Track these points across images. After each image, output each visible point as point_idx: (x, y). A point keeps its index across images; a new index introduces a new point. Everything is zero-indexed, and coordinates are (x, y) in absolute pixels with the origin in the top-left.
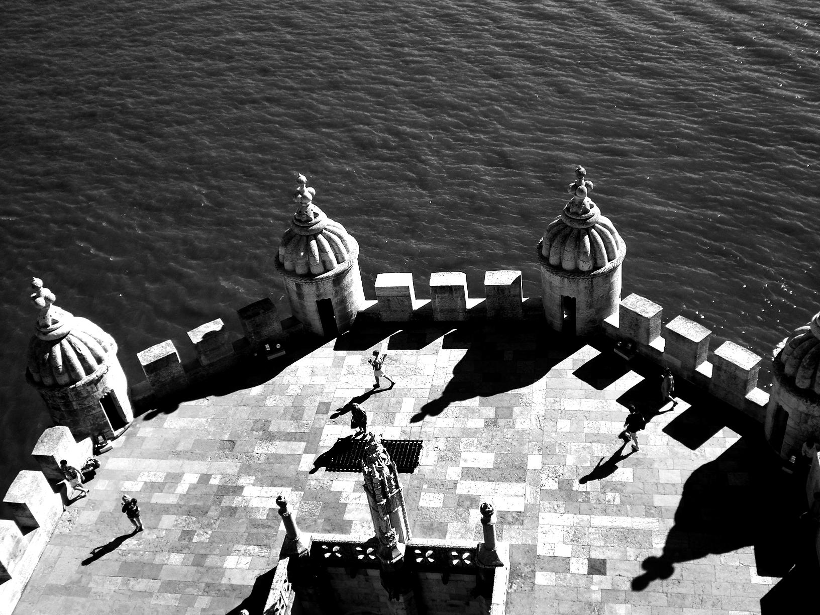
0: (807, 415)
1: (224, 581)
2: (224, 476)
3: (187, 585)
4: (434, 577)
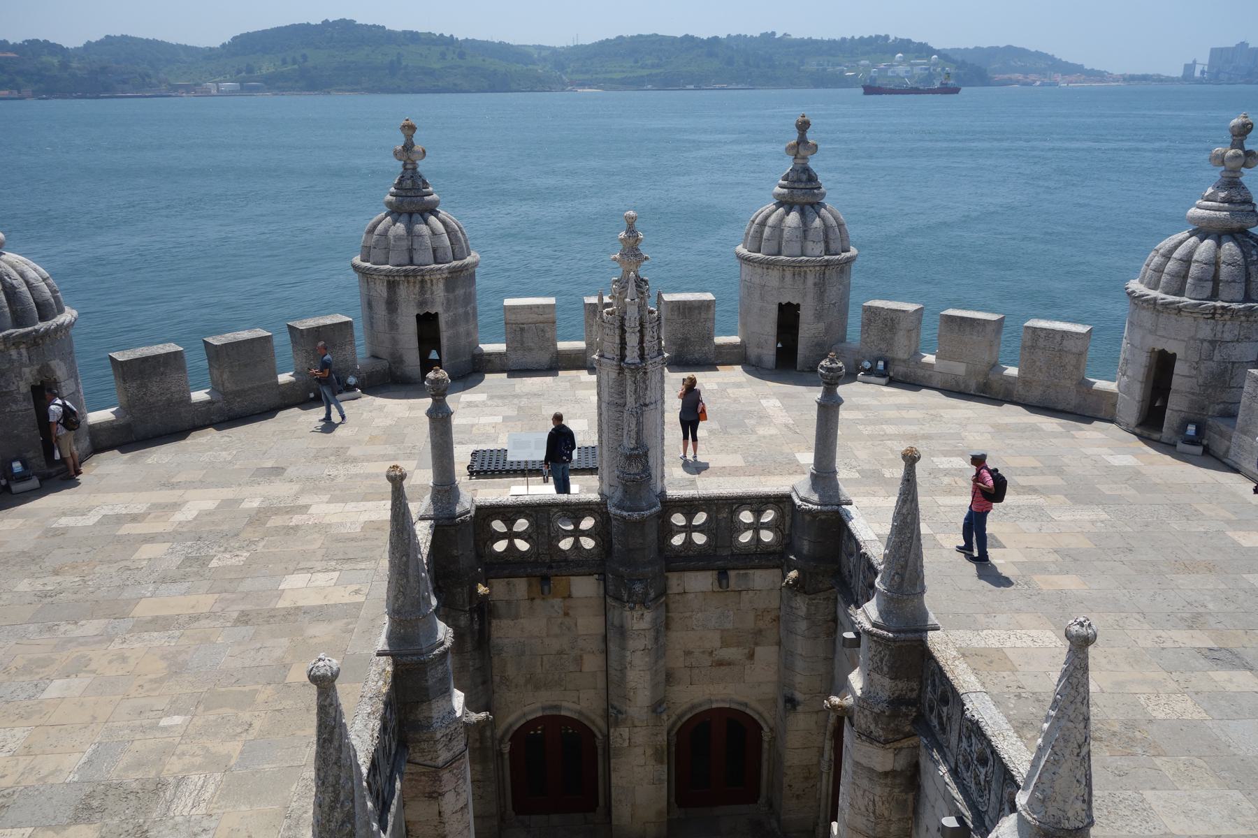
0: (1213, 343)
1: (282, 604)
2: (266, 498)
3: (195, 618)
4: (700, 582)
